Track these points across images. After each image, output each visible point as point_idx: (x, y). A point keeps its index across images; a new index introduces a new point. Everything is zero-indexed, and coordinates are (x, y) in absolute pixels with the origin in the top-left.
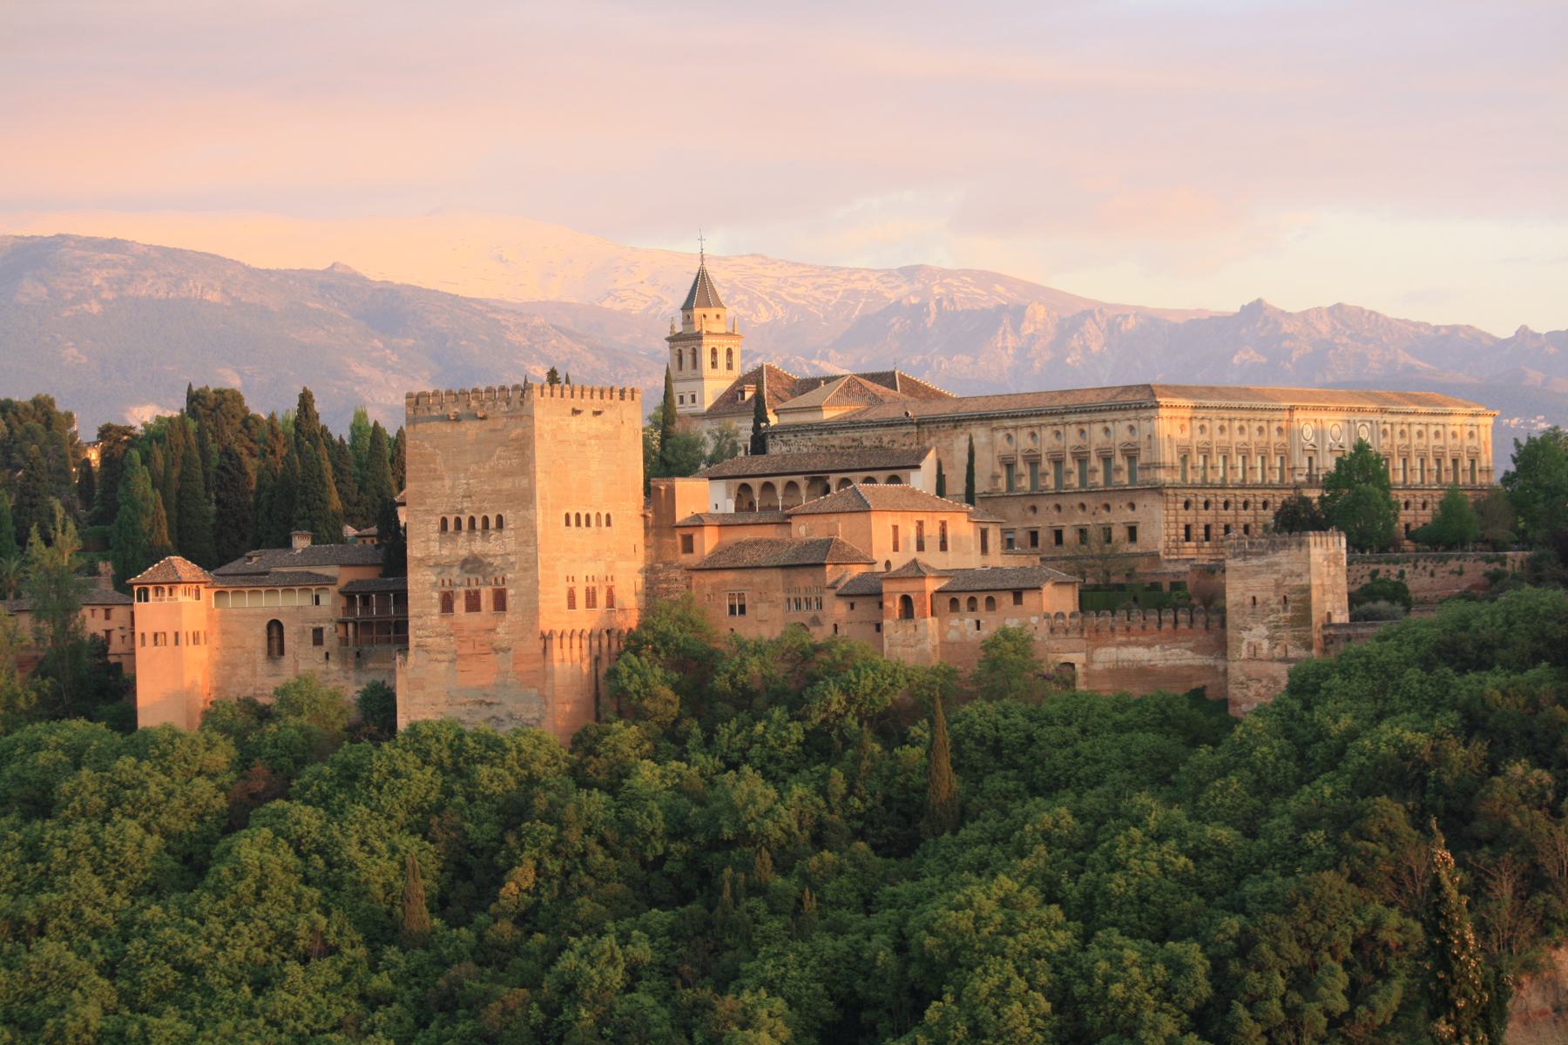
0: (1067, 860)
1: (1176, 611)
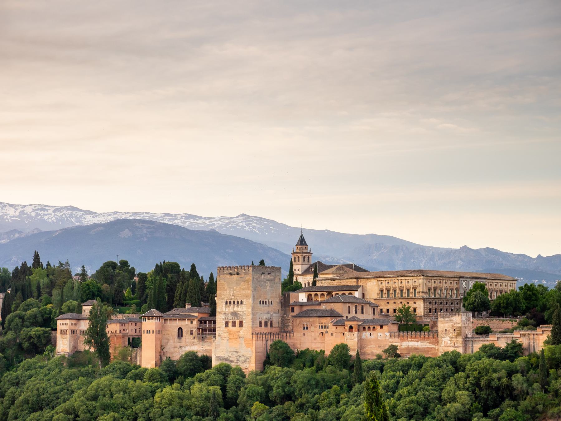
1: (287, 333)
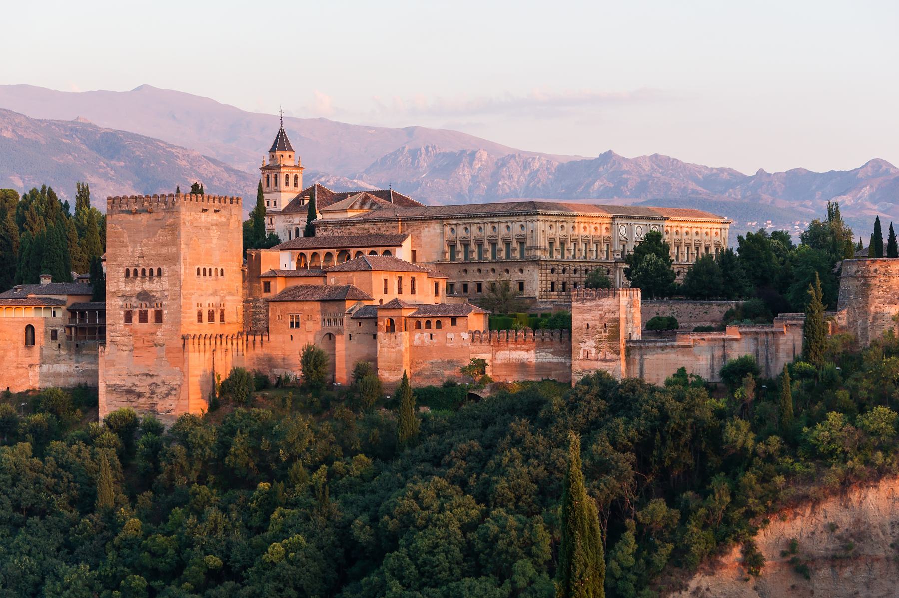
0: (209, 450)
